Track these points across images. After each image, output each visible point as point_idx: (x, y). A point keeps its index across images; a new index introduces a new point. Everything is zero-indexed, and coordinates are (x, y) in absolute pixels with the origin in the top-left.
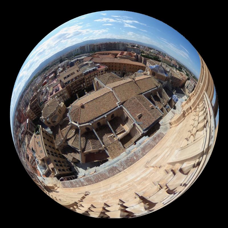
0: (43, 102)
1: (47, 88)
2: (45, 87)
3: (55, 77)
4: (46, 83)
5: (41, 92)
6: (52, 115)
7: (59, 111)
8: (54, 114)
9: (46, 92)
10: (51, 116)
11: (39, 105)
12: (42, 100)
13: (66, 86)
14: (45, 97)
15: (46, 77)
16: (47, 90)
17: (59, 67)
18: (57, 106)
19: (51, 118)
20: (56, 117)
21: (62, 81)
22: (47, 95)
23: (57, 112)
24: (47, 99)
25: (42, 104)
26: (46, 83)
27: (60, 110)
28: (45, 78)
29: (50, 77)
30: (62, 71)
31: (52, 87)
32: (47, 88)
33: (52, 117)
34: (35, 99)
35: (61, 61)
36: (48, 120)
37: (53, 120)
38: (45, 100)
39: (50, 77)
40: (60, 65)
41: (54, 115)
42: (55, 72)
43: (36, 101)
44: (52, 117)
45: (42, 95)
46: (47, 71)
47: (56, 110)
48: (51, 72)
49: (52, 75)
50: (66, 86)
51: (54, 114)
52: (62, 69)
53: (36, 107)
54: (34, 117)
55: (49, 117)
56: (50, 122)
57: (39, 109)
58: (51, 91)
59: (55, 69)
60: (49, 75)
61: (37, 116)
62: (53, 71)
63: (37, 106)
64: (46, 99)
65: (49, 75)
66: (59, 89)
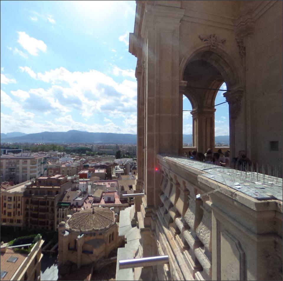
0: (69, 203)
1: (89, 187)
2: (86, 181)
3: (108, 177)
4: (83, 176)
5: (74, 186)
6: (94, 234)
7: (110, 236)
8: (101, 234)
9: (85, 193)
10: (92, 233)
11: (56, 204)
12: (69, 199)
13: (130, 202)
14: (80, 199)
15: (88, 166)
16: (87, 189)
17: (116, 164)
18: (113, 223)
19: (88, 238)
20: (98, 242)
21: (125, 190)
22: (85, 198)
23: (107, 235)
24: (83, 205)
25: (67, 207)
26: (83, 176)
27: (113, 234)
28: (86, 167)
29: (96, 171)
30: (122, 174)
31: (101, 191)
32: (89, 187)
33: (93, 238)
34: (51, 185)
35: (119, 155)
36: (79, 237)
37: (88, 247)
38: (77, 204)
39: (96, 171)
40: (117, 161)
41: (98, 237)
42: (108, 168)
43: (54, 192)
44: (93, 238)
45: (72, 190)
46: (90, 157)
47: (107, 229)
48: (98, 164)
49: (102, 171)
50: (130, 202)
51: (101, 234)
52: (122, 170)
53: (43, 203)
54: (12, 221)
55: (86, 234)
56: (79, 244)
57: (48, 211)
58: (98, 194)
59: (107, 163)
60: (97, 167)
61: (26, 222)
62: (103, 163)
63: (50, 203)
64: (80, 204)
65: (93, 165)
66: (115, 200)
